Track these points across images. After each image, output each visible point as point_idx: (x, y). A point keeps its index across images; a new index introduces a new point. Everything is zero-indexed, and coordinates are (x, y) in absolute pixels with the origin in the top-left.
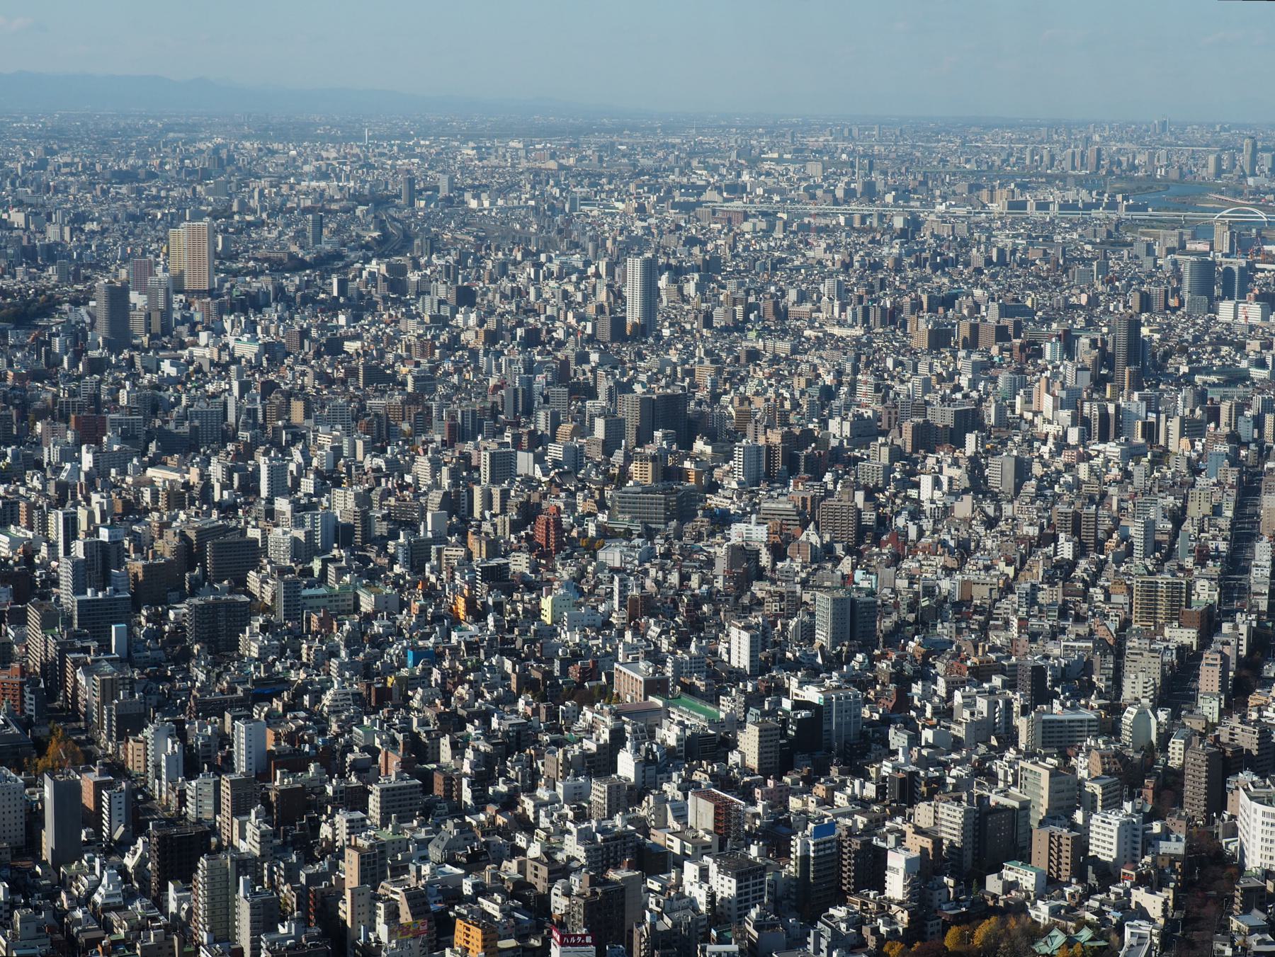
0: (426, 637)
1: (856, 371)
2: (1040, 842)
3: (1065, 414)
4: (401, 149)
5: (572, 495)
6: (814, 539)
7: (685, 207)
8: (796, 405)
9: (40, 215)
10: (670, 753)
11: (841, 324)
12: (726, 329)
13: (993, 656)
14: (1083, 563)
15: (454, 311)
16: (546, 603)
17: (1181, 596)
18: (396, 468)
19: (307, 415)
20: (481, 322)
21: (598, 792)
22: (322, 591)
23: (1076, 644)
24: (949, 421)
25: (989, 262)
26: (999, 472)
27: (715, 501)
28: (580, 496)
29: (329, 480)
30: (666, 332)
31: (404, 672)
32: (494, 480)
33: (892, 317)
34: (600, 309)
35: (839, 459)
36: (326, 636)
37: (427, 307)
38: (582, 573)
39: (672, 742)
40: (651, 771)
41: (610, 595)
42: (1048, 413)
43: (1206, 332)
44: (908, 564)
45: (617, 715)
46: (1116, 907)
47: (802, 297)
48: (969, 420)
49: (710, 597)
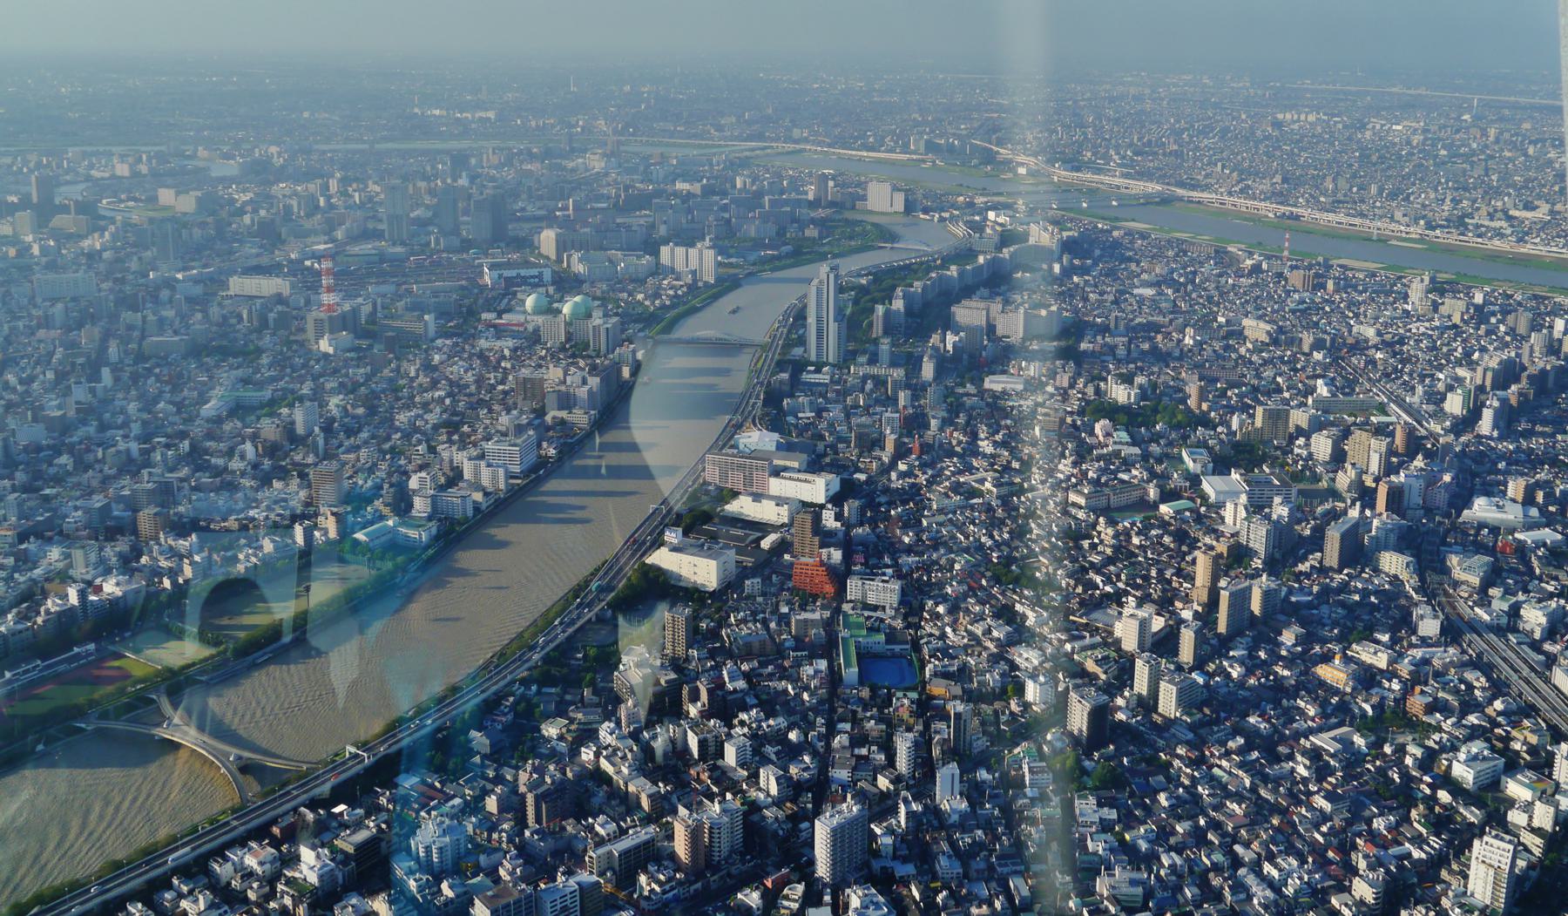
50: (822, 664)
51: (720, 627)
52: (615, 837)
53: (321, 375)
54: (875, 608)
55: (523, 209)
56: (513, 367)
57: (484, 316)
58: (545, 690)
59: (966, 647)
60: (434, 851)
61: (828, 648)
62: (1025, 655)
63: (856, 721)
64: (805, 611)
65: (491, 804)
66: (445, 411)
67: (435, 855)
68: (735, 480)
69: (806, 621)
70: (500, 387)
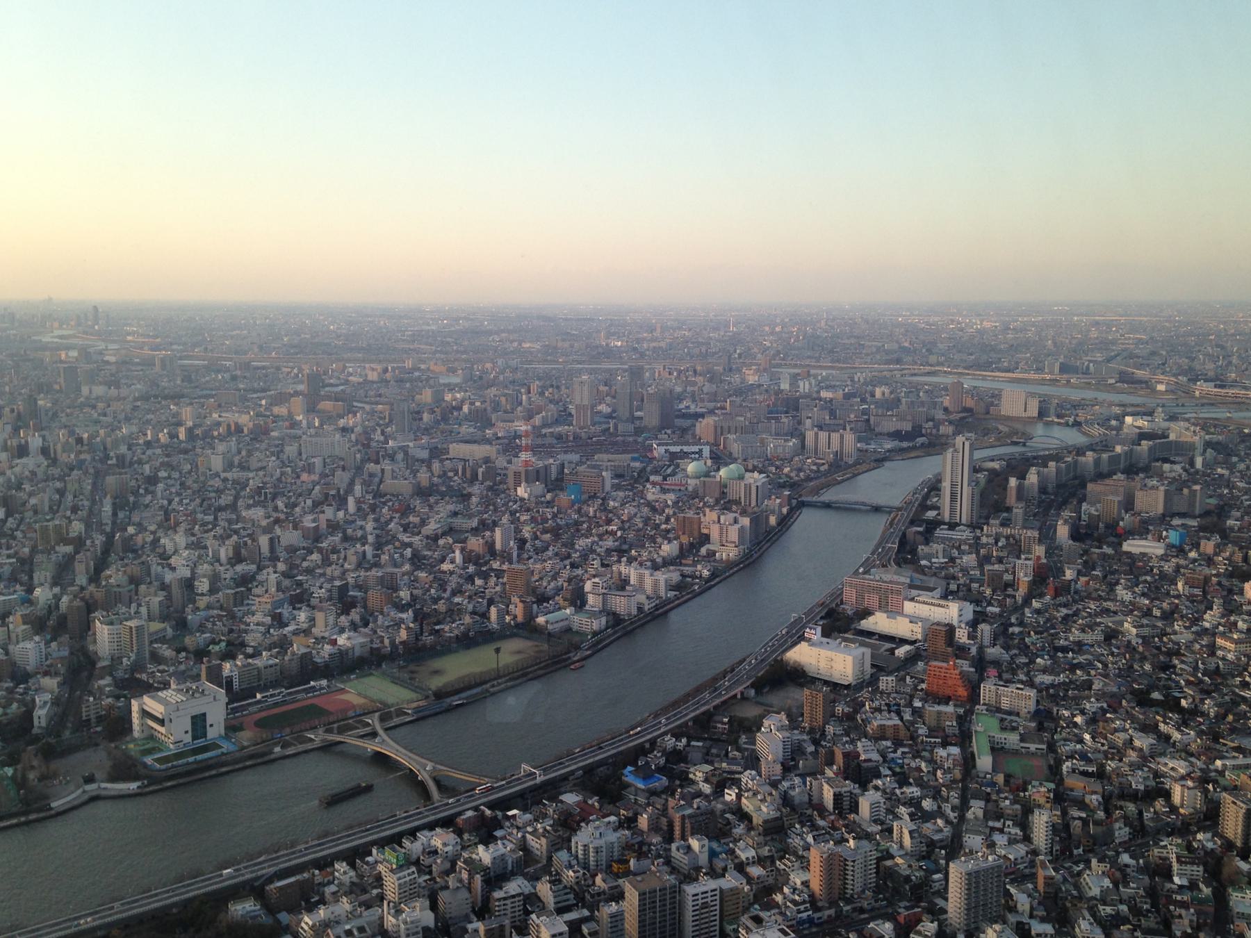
23: (8, 561)
50: (955, 750)
51: (856, 711)
52: (754, 862)
54: (1010, 713)
55: (688, 407)
56: (675, 514)
57: (652, 478)
58: (693, 743)
59: (1105, 753)
60: (591, 850)
61: (964, 738)
62: (1171, 765)
63: (987, 799)
64: (939, 704)
65: (643, 821)
66: (616, 541)
67: (591, 854)
68: (872, 600)
69: (939, 713)
70: (663, 526)
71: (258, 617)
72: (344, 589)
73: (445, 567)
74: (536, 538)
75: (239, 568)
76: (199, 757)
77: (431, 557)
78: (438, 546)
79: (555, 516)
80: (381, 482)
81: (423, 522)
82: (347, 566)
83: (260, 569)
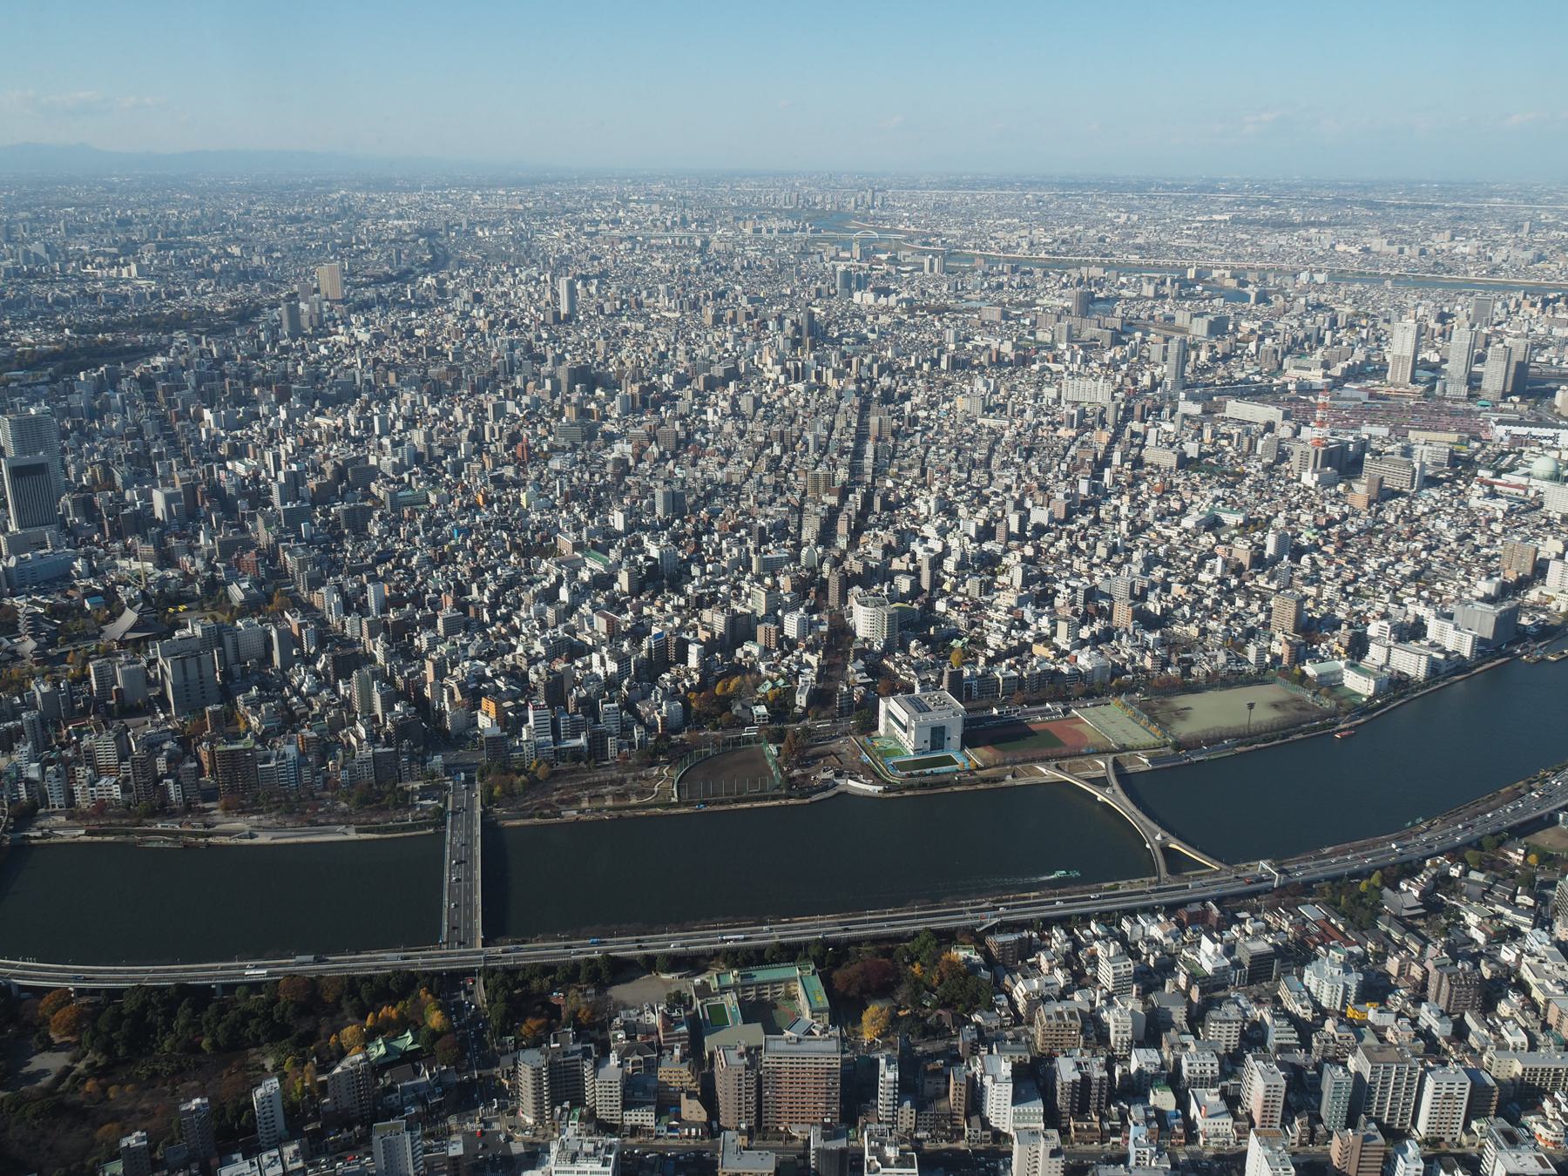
0: (463, 518)
1: (676, 340)
2: (760, 630)
3: (778, 368)
4: (442, 197)
5: (535, 425)
6: (655, 450)
7: (590, 235)
8: (647, 363)
9: (248, 249)
10: (585, 585)
11: (668, 310)
12: (612, 315)
13: (741, 518)
14: (785, 458)
15: (472, 308)
16: (523, 496)
17: (830, 480)
18: (445, 413)
19: (397, 380)
20: (486, 316)
21: (550, 613)
22: (410, 493)
24: (722, 374)
25: (743, 268)
26: (745, 404)
27: (607, 427)
28: (539, 426)
29: (411, 423)
30: (581, 318)
31: (453, 542)
32: (496, 419)
33: (695, 306)
34: (548, 304)
35: (670, 398)
36: (412, 520)
37: (458, 304)
38: (541, 474)
39: (586, 579)
40: (576, 596)
41: (555, 489)
42: (770, 366)
43: (847, 310)
44: (701, 462)
45: (558, 565)
46: (796, 663)
47: (649, 296)
48: (733, 374)
49: (605, 488)
53: (1298, 507)
56: (1504, 531)
57: (1481, 473)
65: (1392, 965)
70: (1485, 551)
71: (1001, 615)
72: (1092, 594)
73: (1204, 576)
74: (1317, 547)
75: (987, 546)
76: (935, 770)
77: (1189, 559)
78: (1198, 544)
79: (1345, 517)
80: (1142, 446)
81: (1183, 511)
82: (1096, 560)
83: (1007, 551)
